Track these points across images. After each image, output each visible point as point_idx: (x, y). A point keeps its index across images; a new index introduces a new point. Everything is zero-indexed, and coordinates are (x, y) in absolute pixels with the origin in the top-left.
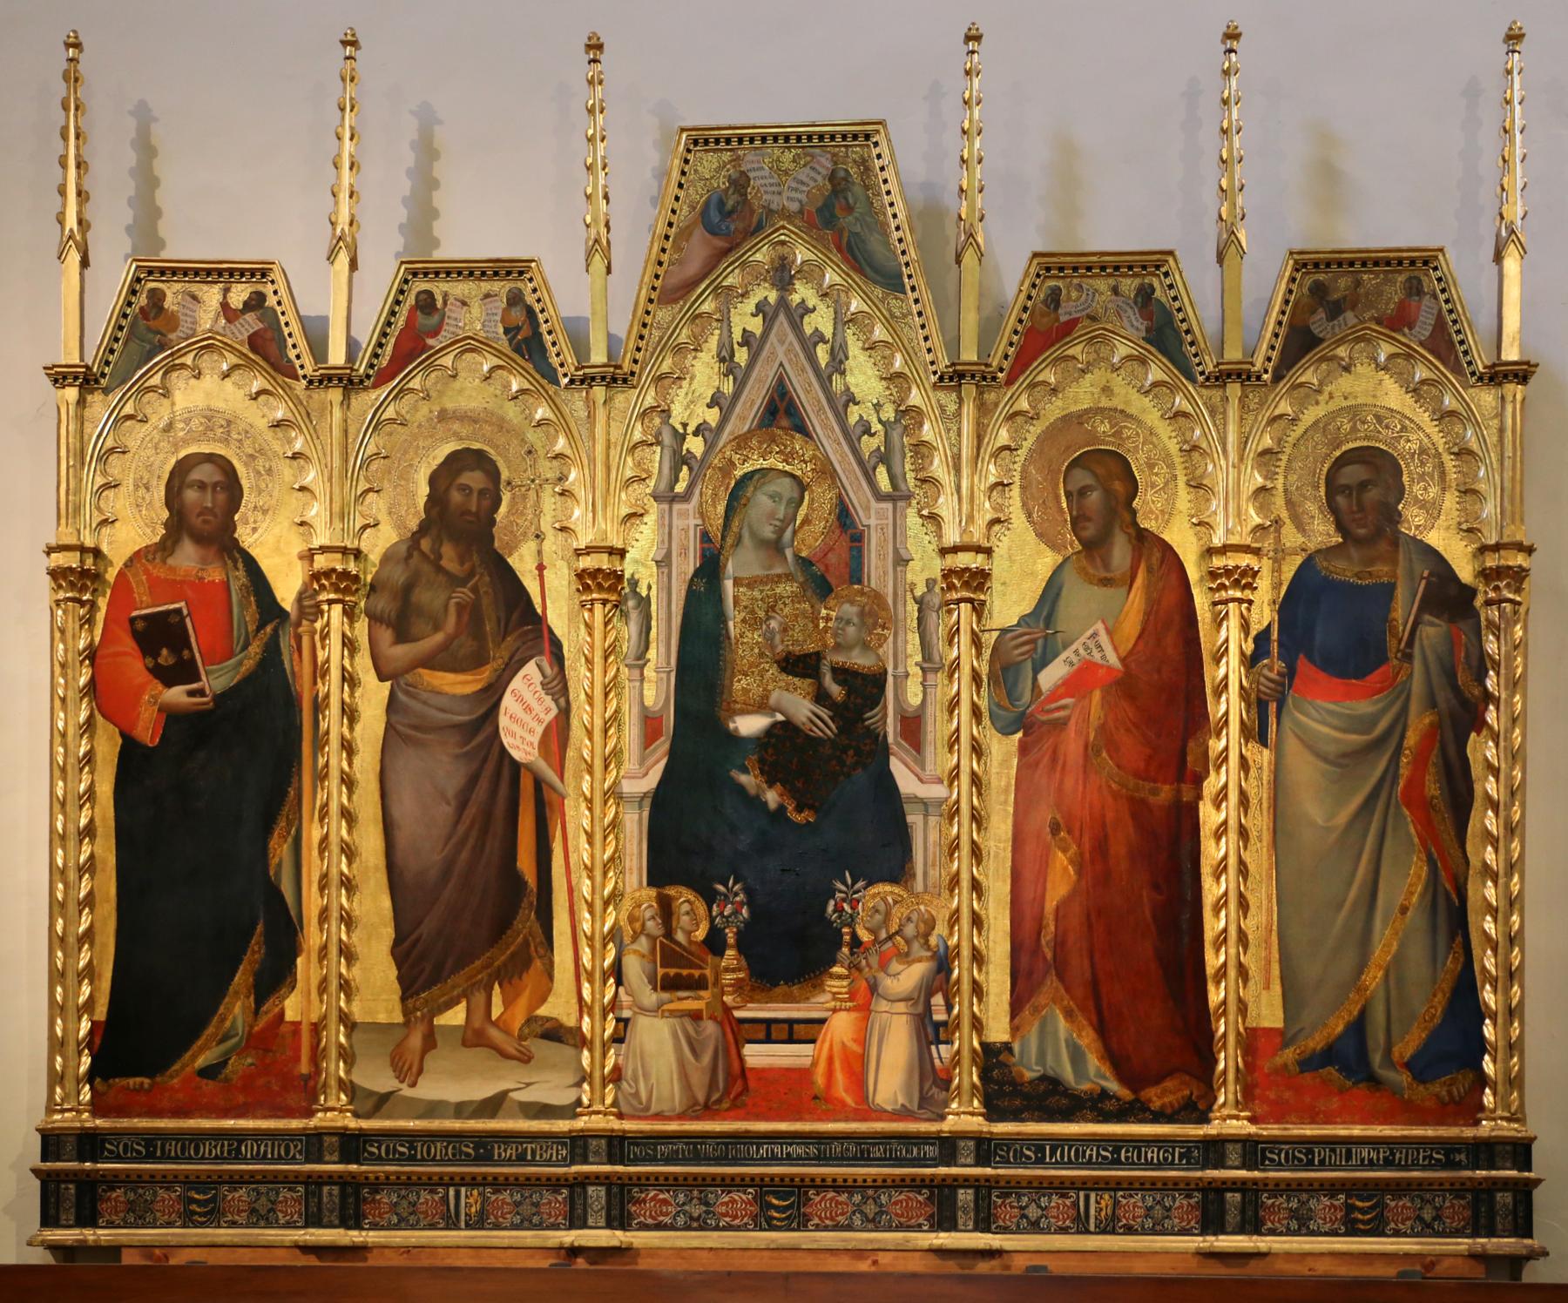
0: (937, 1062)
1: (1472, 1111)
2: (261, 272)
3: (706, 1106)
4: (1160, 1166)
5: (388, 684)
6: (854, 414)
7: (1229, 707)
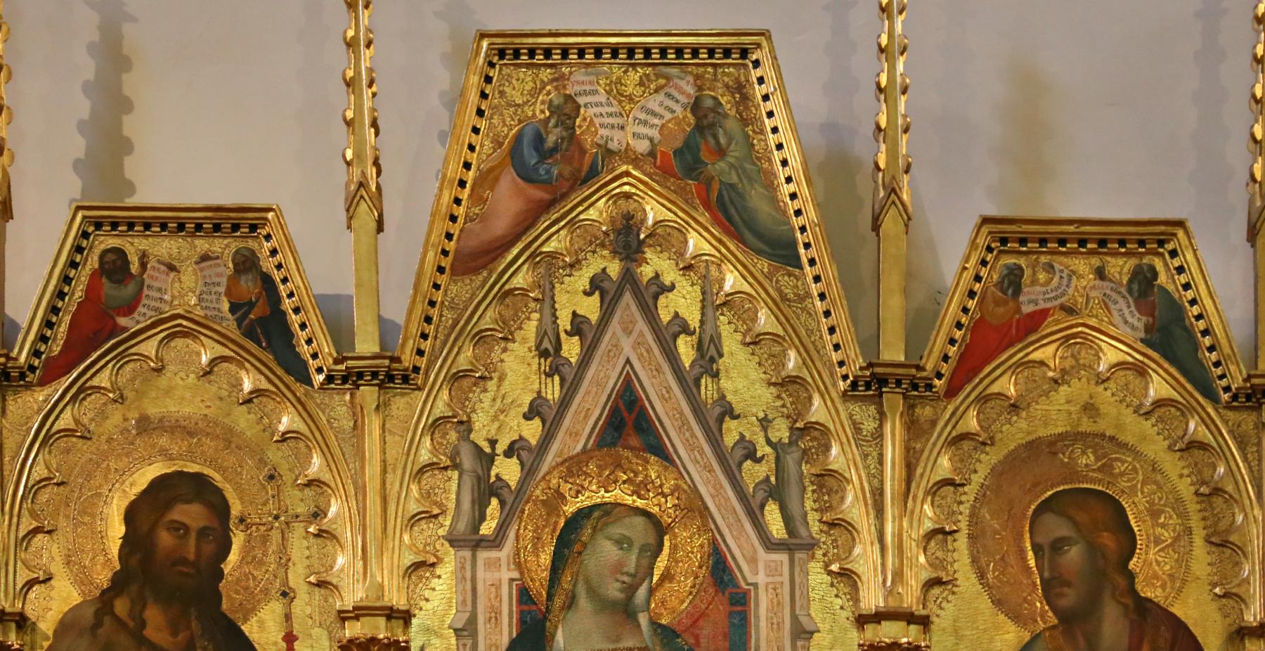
6: (732, 432)
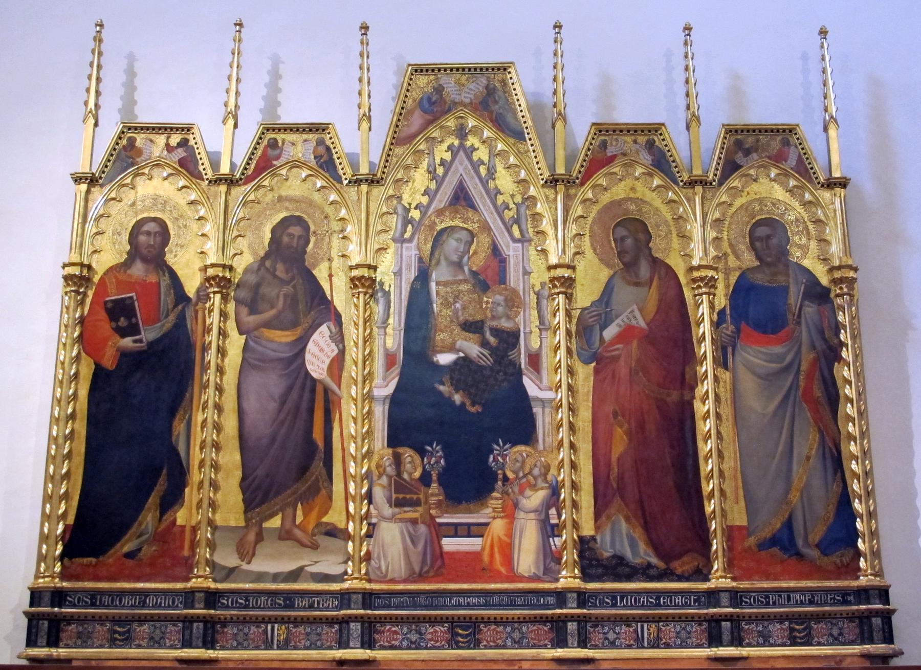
0: (553, 547)
1: (855, 572)
2: (188, 129)
3: (420, 575)
4: (683, 606)
5: (244, 336)
6: (500, 199)
7: (706, 348)
